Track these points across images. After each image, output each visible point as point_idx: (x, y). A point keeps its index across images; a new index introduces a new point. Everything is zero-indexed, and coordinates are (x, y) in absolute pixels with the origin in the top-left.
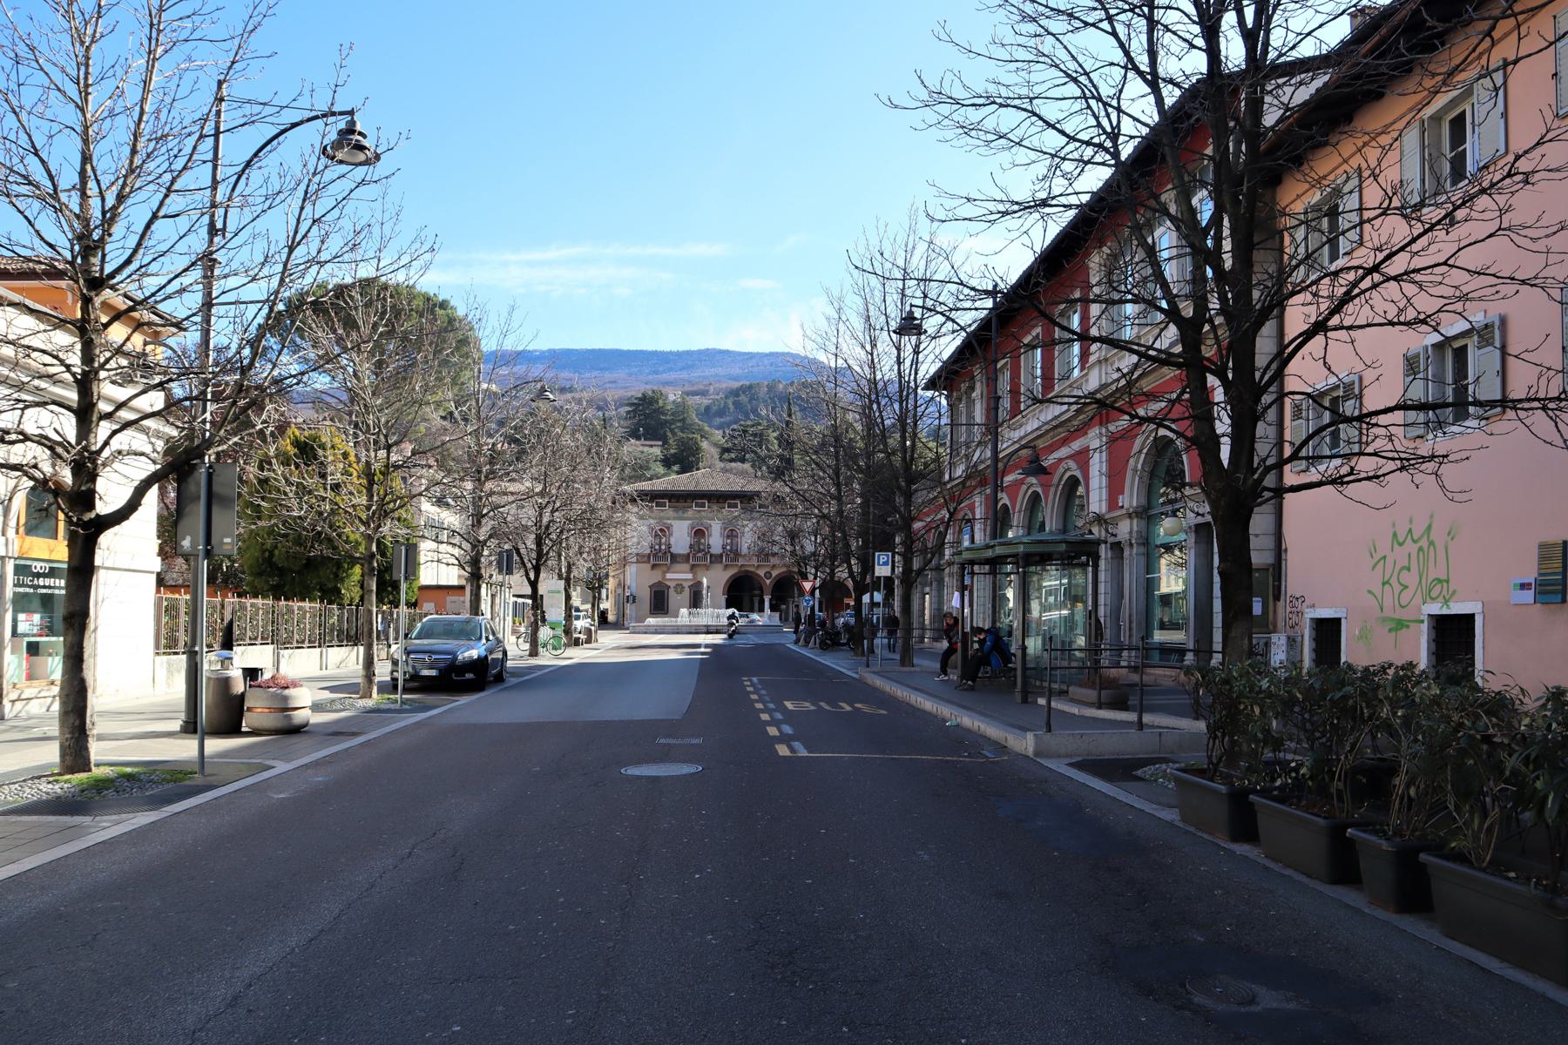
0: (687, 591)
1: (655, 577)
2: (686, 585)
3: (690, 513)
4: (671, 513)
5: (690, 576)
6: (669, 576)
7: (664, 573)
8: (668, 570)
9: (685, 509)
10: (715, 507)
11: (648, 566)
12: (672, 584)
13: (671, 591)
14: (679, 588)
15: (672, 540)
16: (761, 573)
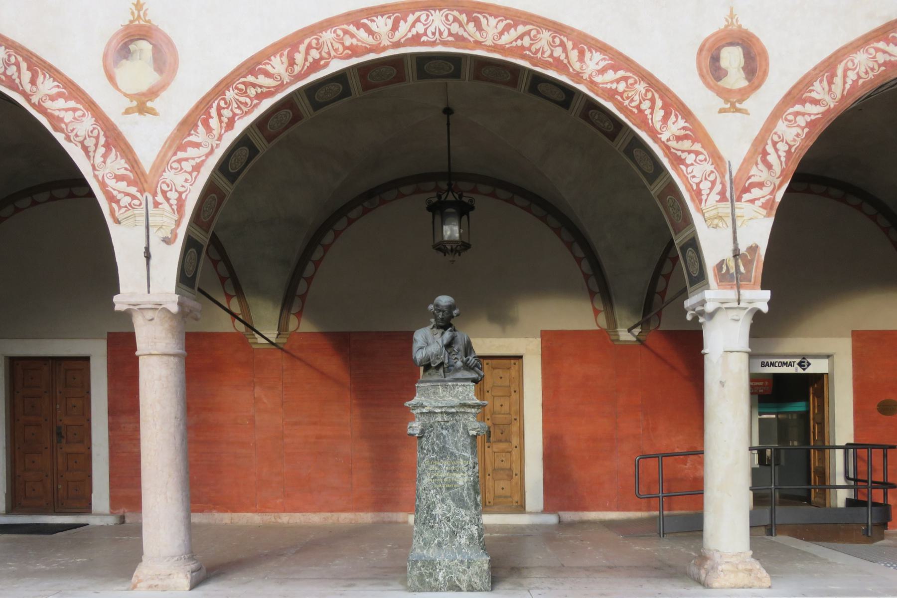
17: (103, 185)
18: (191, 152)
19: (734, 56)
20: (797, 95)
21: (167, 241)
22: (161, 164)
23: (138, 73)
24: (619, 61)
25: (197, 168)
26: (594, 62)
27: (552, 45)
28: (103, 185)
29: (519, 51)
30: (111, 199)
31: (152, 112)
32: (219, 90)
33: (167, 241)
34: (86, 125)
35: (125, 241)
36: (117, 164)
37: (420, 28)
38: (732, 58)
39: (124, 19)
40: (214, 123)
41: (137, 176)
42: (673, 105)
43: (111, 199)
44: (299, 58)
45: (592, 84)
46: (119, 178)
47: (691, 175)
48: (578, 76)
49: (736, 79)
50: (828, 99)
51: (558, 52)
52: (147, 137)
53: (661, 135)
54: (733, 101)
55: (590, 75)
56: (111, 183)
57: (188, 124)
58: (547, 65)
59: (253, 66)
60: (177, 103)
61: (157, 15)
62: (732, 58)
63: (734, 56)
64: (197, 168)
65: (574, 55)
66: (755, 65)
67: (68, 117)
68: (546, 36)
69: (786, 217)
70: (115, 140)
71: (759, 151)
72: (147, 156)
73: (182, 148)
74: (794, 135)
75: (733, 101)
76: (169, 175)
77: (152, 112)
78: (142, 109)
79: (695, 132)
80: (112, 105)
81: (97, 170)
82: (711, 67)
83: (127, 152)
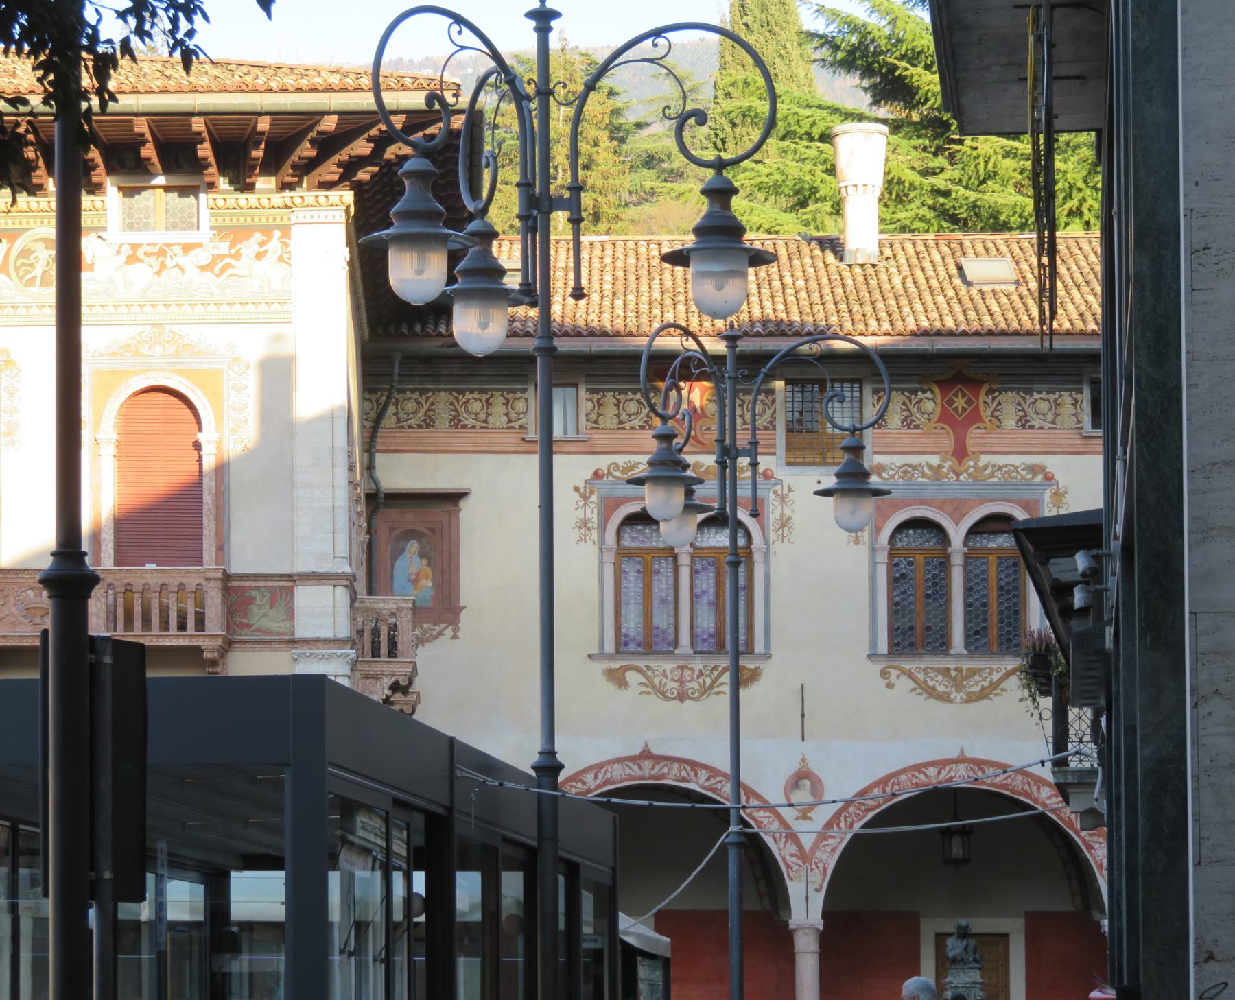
17: (784, 859)
18: (830, 841)
21: (817, 890)
22: (815, 847)
23: (802, 796)
25: (833, 850)
27: (1023, 783)
28: (784, 859)
29: (1005, 786)
30: (788, 866)
31: (810, 819)
33: (817, 890)
34: (775, 825)
35: (795, 890)
36: (792, 848)
37: (952, 774)
40: (842, 825)
41: (803, 855)
43: (788, 866)
44: (888, 789)
45: (1044, 805)
46: (792, 855)
48: (1036, 801)
51: (1026, 787)
52: (808, 832)
56: (788, 858)
58: (1019, 794)
60: (823, 814)
61: (814, 766)
64: (833, 850)
65: (1034, 789)
67: (765, 821)
68: (1020, 778)
70: (792, 836)
72: (807, 841)
73: (826, 839)
76: (818, 854)
77: (810, 819)
78: (805, 817)
80: (788, 814)
81: (781, 851)
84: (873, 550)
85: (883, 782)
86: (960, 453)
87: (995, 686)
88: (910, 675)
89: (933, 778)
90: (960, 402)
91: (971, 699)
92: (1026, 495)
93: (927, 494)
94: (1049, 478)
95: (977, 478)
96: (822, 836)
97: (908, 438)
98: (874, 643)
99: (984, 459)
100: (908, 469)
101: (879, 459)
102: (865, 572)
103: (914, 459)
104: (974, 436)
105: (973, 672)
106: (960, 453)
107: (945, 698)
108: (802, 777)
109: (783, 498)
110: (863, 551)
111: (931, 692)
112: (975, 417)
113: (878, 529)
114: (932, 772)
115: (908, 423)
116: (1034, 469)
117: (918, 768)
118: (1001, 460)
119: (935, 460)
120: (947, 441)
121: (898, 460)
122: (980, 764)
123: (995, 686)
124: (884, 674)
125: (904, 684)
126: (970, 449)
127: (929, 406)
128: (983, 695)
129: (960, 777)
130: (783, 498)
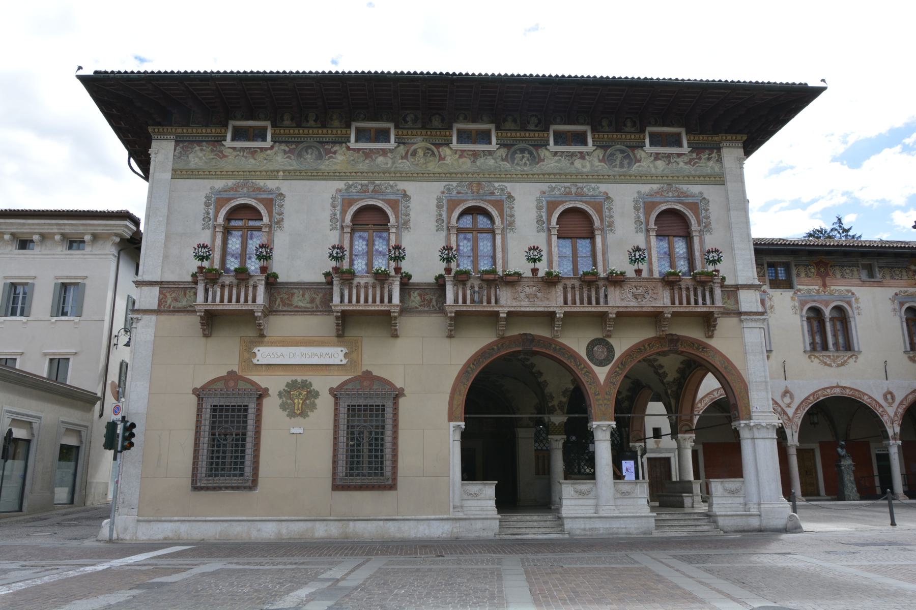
0: (325, 403)
1: (215, 359)
2: (323, 384)
3: (340, 159)
4: (279, 159)
5: (335, 355)
6: (265, 354)
7: (248, 347)
8: (261, 337)
9: (324, 147)
10: (419, 144)
11: (193, 322)
12: (274, 384)
13: (271, 408)
14: (299, 397)
15: (281, 242)
16: (577, 343)
19: (889, 395)
20: (901, 403)
23: (787, 400)
24: (870, 397)
26: (866, 397)
32: (802, 403)
38: (889, 396)
39: (783, 390)
42: (880, 406)
47: (885, 419)
49: (890, 400)
50: (906, 404)
53: (879, 411)
54: (890, 405)
55: (866, 400)
57: (797, 410)
59: (807, 398)
62: (889, 396)
63: (889, 395)
66: (893, 398)
69: (902, 426)
71: (896, 414)
72: (791, 415)
74: (901, 411)
75: (890, 405)
79: (884, 411)
82: (886, 399)
83: (787, 415)
84: (802, 316)
85: (813, 394)
86: (824, 285)
87: (845, 361)
88: (818, 358)
89: (830, 393)
90: (822, 270)
91: (838, 366)
92: (848, 299)
93: (816, 298)
94: (853, 294)
95: (831, 294)
96: (795, 413)
97: (807, 280)
98: (805, 347)
99: (832, 288)
100: (809, 291)
101: (799, 287)
102: (799, 323)
103: (811, 287)
104: (828, 280)
105: (838, 357)
106: (824, 285)
107: (830, 365)
108: (786, 392)
109: (770, 299)
110: (798, 317)
111: (826, 364)
112: (827, 275)
113: (802, 310)
114: (829, 390)
115: (807, 275)
116: (848, 291)
117: (824, 389)
118: (838, 288)
119: (817, 288)
120: (820, 282)
121: (806, 287)
122: (844, 388)
123: (845, 361)
124: (809, 357)
125: (816, 361)
126: (828, 284)
127: (813, 270)
128: (842, 364)
129: (837, 392)
130: (770, 299)
